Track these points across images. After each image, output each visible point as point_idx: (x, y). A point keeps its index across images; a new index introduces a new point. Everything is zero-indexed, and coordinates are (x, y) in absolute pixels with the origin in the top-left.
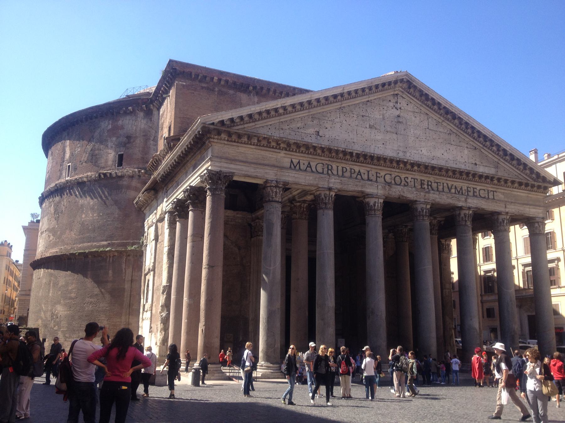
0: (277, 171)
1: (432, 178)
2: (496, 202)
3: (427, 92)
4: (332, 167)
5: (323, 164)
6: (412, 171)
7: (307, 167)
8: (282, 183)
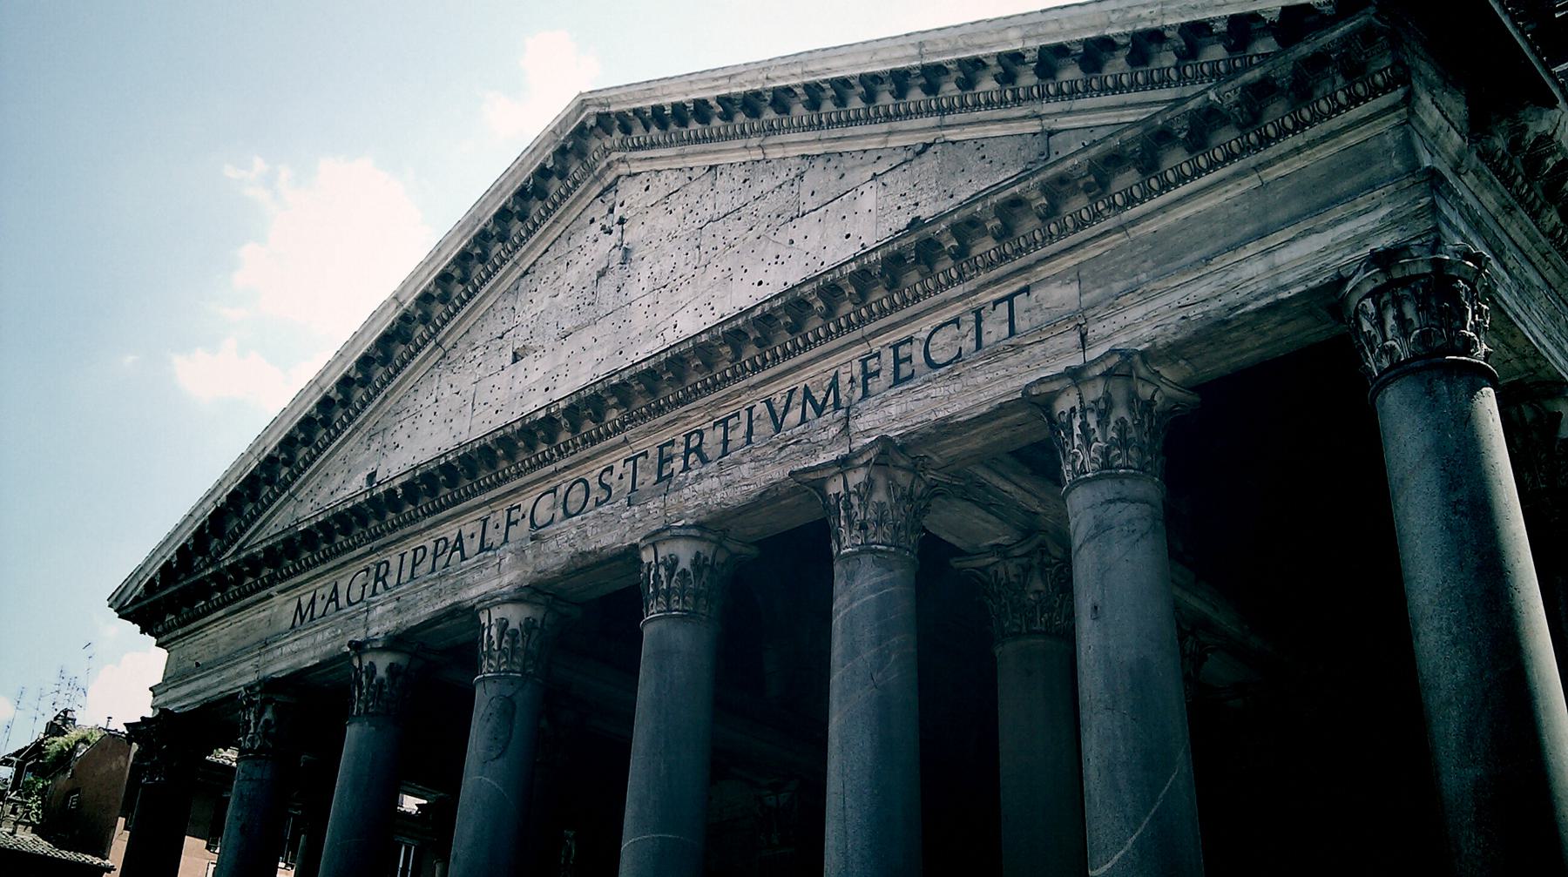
0: (259, 655)
1: (695, 415)
2: (1017, 348)
3: (653, 103)
4: (387, 563)
5: (367, 570)
6: (609, 434)
7: (330, 600)
8: (258, 689)
